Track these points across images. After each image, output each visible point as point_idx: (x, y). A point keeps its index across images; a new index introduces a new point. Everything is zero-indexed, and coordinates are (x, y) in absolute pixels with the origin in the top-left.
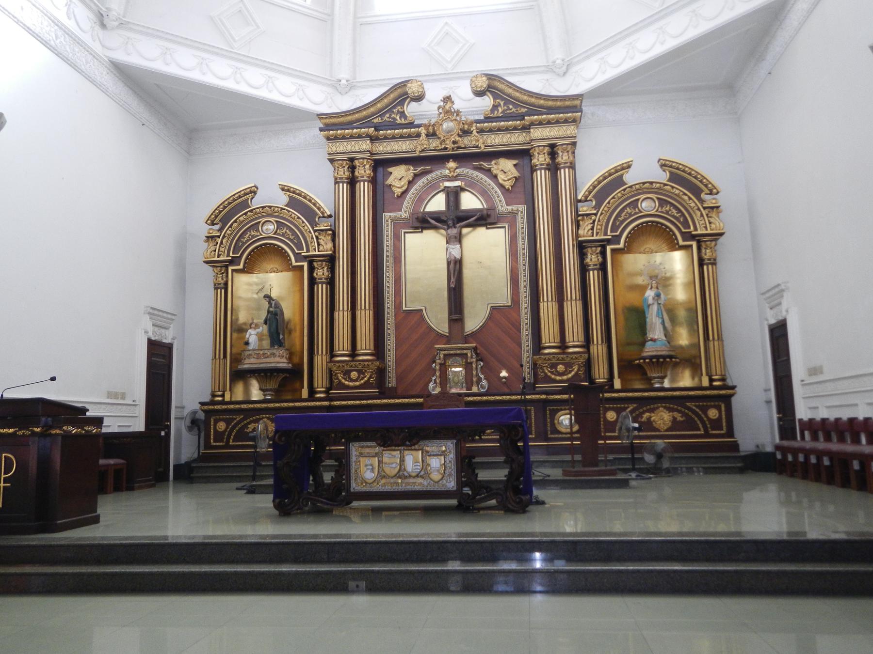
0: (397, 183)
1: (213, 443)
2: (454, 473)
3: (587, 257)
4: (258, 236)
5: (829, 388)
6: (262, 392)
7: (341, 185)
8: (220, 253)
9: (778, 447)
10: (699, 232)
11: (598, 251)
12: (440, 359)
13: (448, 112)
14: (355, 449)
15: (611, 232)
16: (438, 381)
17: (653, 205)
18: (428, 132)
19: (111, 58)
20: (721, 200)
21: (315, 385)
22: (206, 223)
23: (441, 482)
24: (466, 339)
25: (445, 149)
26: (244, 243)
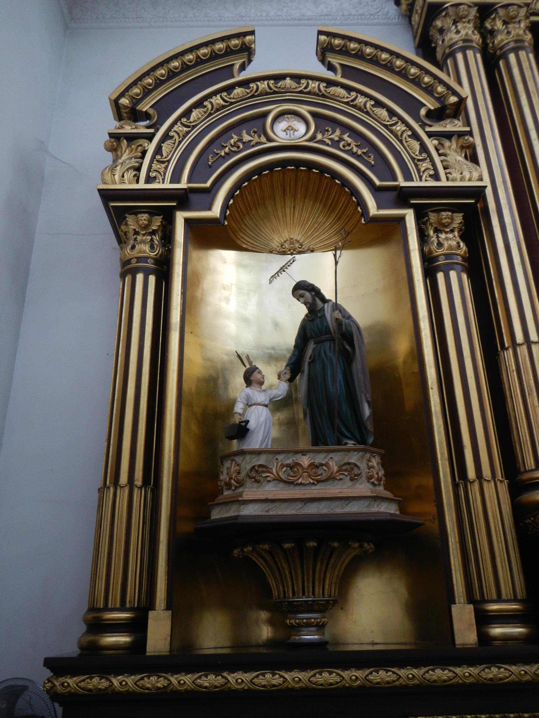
8: (152, 174)
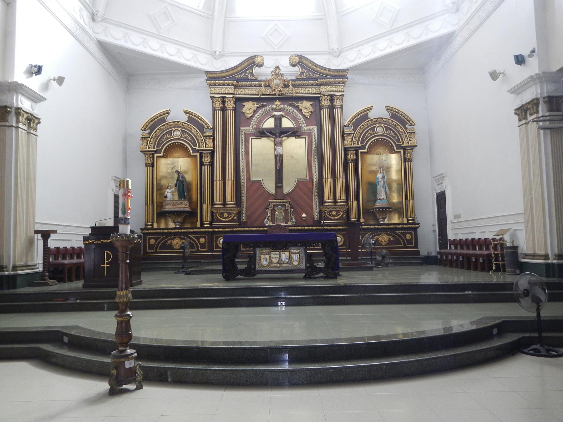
0: (247, 111)
1: (148, 251)
2: (304, 262)
3: (348, 156)
4: (171, 138)
5: (464, 225)
6: (174, 224)
7: (217, 111)
8: (150, 147)
9: (439, 253)
10: (405, 145)
11: (354, 153)
12: (271, 207)
13: (277, 75)
14: (258, 250)
15: (361, 143)
16: (270, 219)
17: (383, 130)
18: (265, 84)
19: (98, 39)
20: (416, 128)
21: (204, 220)
22: (141, 129)
23: (298, 266)
24: (285, 196)
25: (275, 94)
26: (163, 142)
